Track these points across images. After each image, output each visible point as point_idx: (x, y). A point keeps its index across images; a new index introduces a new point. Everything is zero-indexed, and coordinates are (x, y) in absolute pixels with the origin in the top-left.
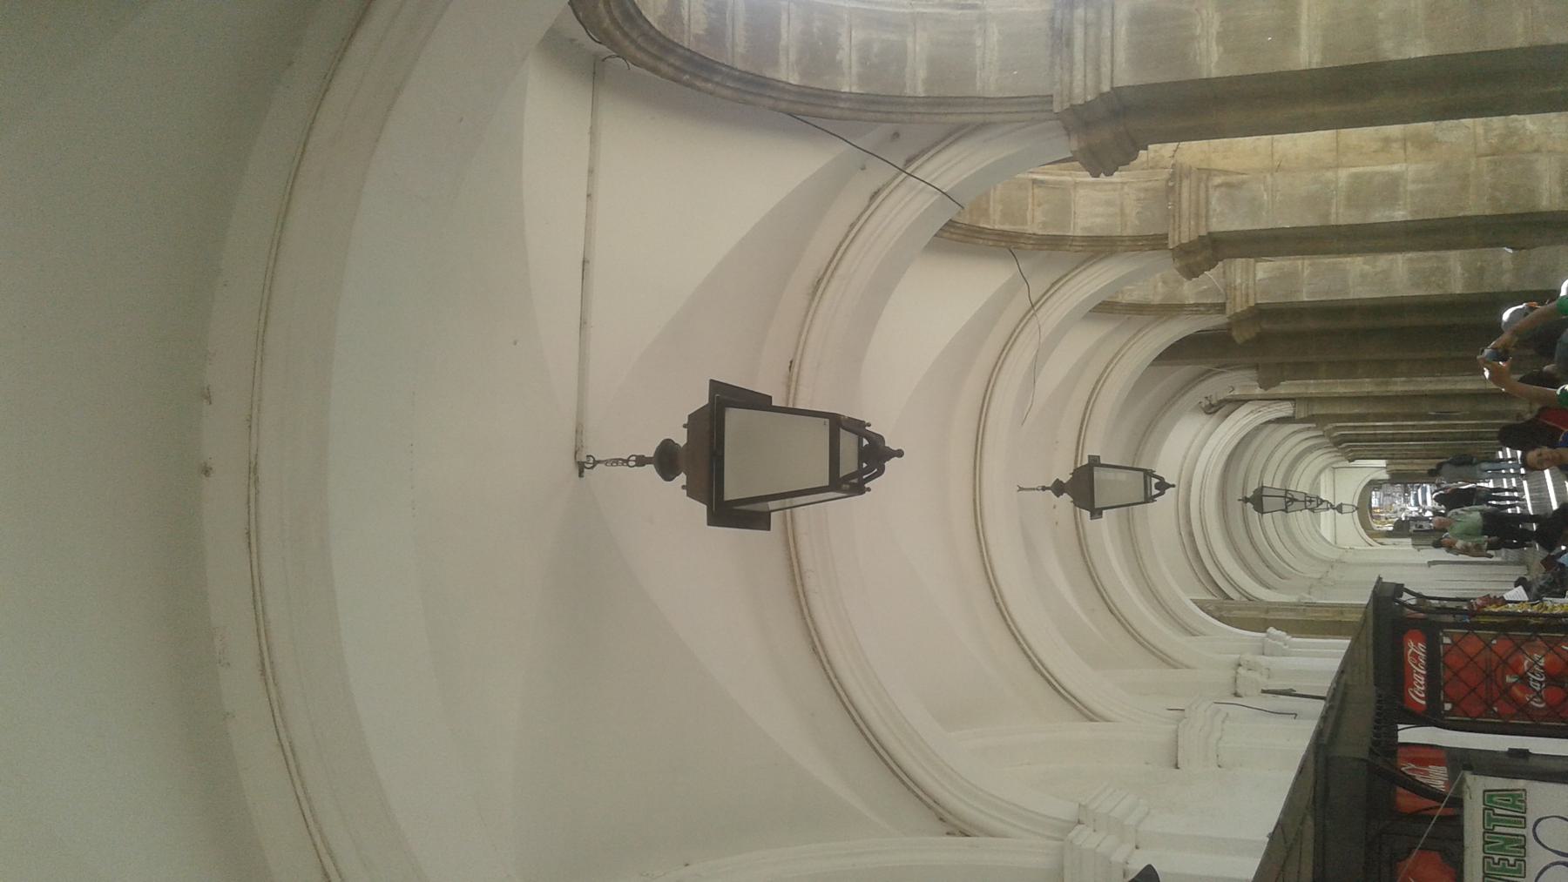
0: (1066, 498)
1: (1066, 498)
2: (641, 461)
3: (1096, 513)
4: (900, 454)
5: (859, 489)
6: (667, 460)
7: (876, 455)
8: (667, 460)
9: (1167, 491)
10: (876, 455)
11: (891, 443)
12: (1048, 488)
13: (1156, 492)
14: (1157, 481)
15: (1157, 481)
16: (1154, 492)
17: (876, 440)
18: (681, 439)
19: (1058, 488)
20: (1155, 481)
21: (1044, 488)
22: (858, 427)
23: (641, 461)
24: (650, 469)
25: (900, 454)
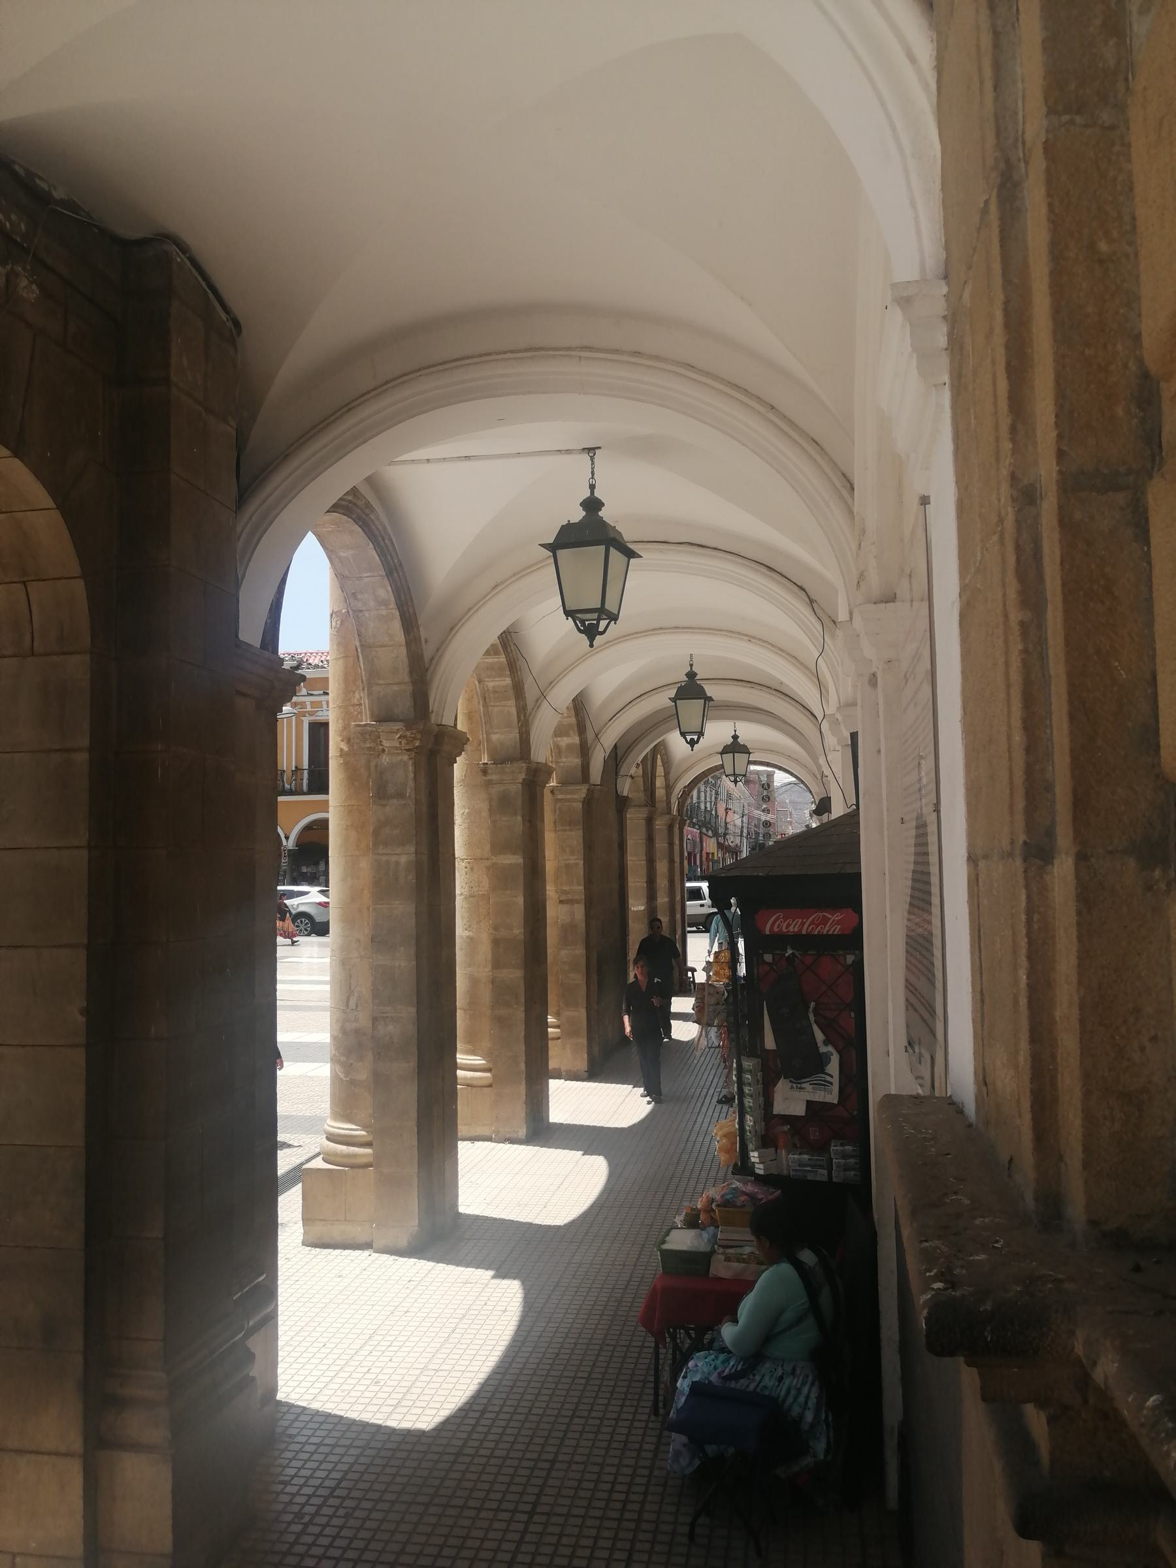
2: (592, 487)
3: (674, 700)
4: (591, 646)
6: (592, 505)
7: (591, 632)
8: (592, 505)
11: (599, 640)
12: (691, 668)
14: (696, 740)
15: (696, 740)
16: (689, 738)
19: (691, 675)
20: (695, 737)
21: (691, 665)
23: (592, 487)
24: (588, 494)
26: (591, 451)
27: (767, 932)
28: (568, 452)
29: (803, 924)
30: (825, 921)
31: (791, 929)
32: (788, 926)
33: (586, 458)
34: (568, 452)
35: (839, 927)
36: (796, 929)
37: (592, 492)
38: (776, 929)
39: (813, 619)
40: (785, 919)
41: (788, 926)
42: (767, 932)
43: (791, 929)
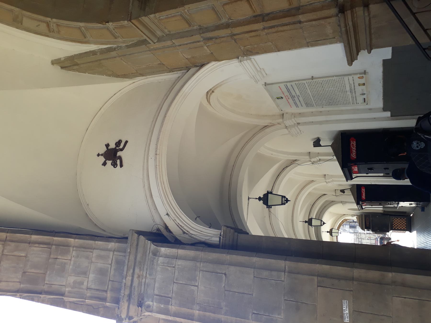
0: (307, 224)
1: (307, 224)
2: (256, 199)
4: (290, 201)
5: (284, 204)
6: (260, 199)
7: (287, 201)
8: (260, 199)
9: (325, 224)
10: (287, 201)
13: (322, 224)
14: (323, 222)
15: (323, 222)
16: (322, 224)
17: (287, 199)
18: (262, 196)
20: (323, 222)
22: (284, 197)
23: (256, 199)
25: (290, 201)
26: (249, 199)
27: (356, 157)
28: (248, 203)
29: (353, 149)
30: (353, 145)
31: (355, 152)
32: (354, 152)
33: (250, 200)
34: (248, 203)
35: (354, 142)
36: (355, 151)
37: (257, 199)
38: (355, 155)
39: (290, 166)
40: (352, 153)
41: (354, 152)
42: (356, 157)
43: (355, 152)
